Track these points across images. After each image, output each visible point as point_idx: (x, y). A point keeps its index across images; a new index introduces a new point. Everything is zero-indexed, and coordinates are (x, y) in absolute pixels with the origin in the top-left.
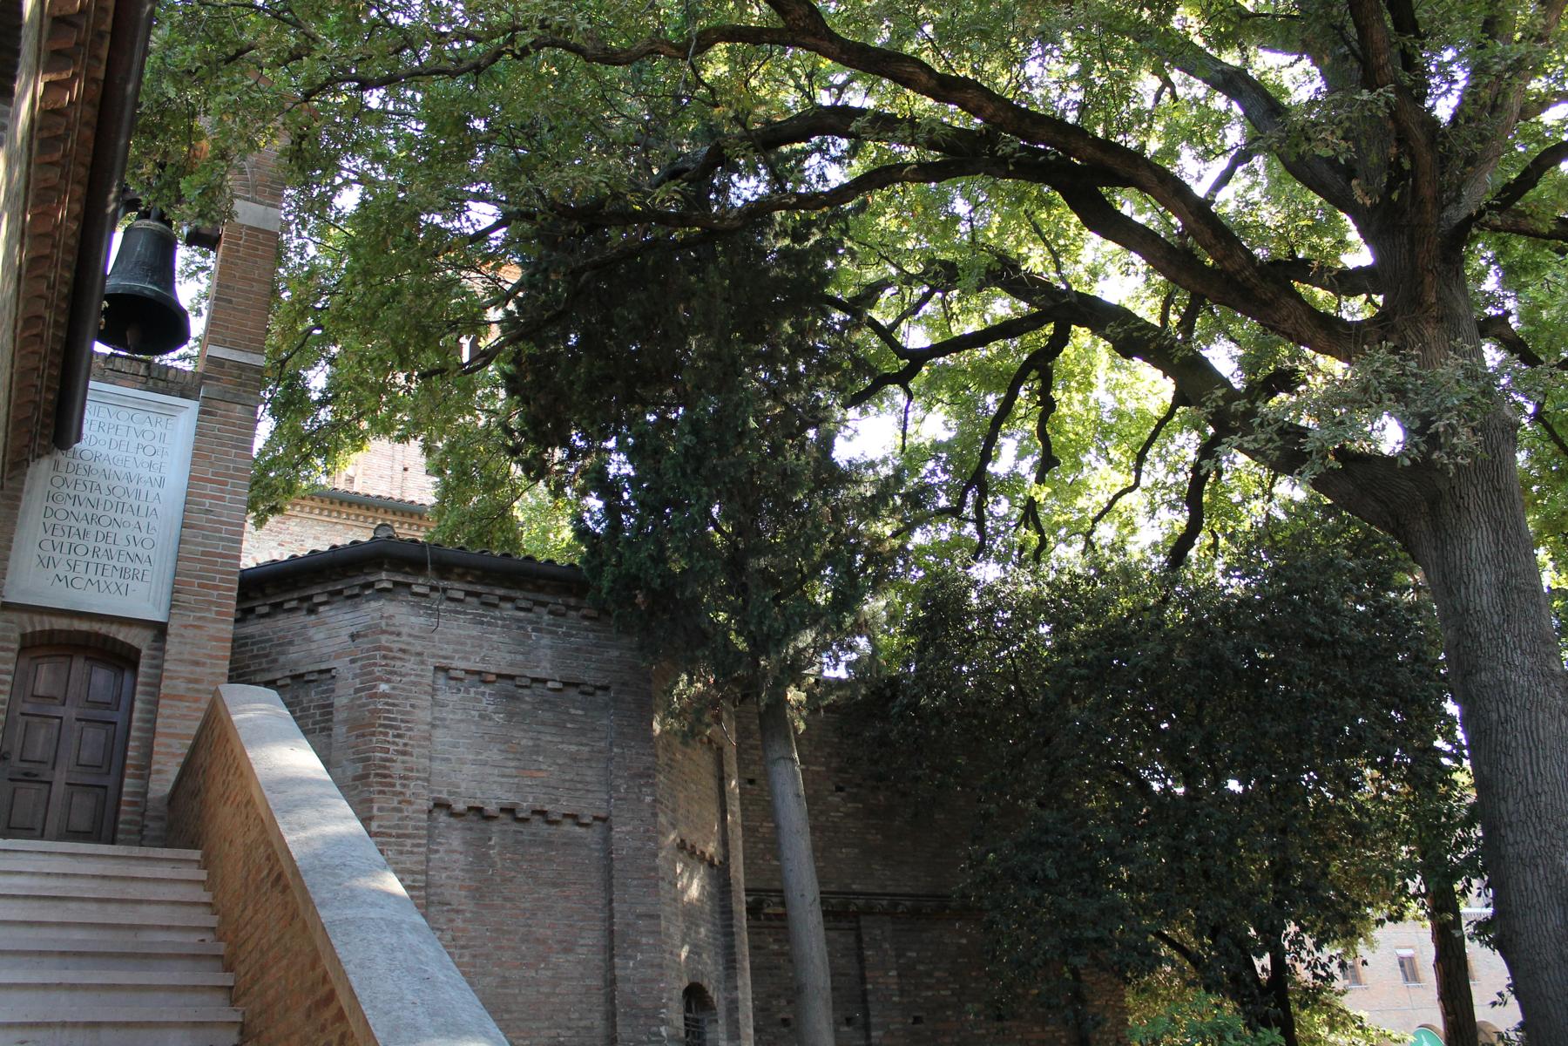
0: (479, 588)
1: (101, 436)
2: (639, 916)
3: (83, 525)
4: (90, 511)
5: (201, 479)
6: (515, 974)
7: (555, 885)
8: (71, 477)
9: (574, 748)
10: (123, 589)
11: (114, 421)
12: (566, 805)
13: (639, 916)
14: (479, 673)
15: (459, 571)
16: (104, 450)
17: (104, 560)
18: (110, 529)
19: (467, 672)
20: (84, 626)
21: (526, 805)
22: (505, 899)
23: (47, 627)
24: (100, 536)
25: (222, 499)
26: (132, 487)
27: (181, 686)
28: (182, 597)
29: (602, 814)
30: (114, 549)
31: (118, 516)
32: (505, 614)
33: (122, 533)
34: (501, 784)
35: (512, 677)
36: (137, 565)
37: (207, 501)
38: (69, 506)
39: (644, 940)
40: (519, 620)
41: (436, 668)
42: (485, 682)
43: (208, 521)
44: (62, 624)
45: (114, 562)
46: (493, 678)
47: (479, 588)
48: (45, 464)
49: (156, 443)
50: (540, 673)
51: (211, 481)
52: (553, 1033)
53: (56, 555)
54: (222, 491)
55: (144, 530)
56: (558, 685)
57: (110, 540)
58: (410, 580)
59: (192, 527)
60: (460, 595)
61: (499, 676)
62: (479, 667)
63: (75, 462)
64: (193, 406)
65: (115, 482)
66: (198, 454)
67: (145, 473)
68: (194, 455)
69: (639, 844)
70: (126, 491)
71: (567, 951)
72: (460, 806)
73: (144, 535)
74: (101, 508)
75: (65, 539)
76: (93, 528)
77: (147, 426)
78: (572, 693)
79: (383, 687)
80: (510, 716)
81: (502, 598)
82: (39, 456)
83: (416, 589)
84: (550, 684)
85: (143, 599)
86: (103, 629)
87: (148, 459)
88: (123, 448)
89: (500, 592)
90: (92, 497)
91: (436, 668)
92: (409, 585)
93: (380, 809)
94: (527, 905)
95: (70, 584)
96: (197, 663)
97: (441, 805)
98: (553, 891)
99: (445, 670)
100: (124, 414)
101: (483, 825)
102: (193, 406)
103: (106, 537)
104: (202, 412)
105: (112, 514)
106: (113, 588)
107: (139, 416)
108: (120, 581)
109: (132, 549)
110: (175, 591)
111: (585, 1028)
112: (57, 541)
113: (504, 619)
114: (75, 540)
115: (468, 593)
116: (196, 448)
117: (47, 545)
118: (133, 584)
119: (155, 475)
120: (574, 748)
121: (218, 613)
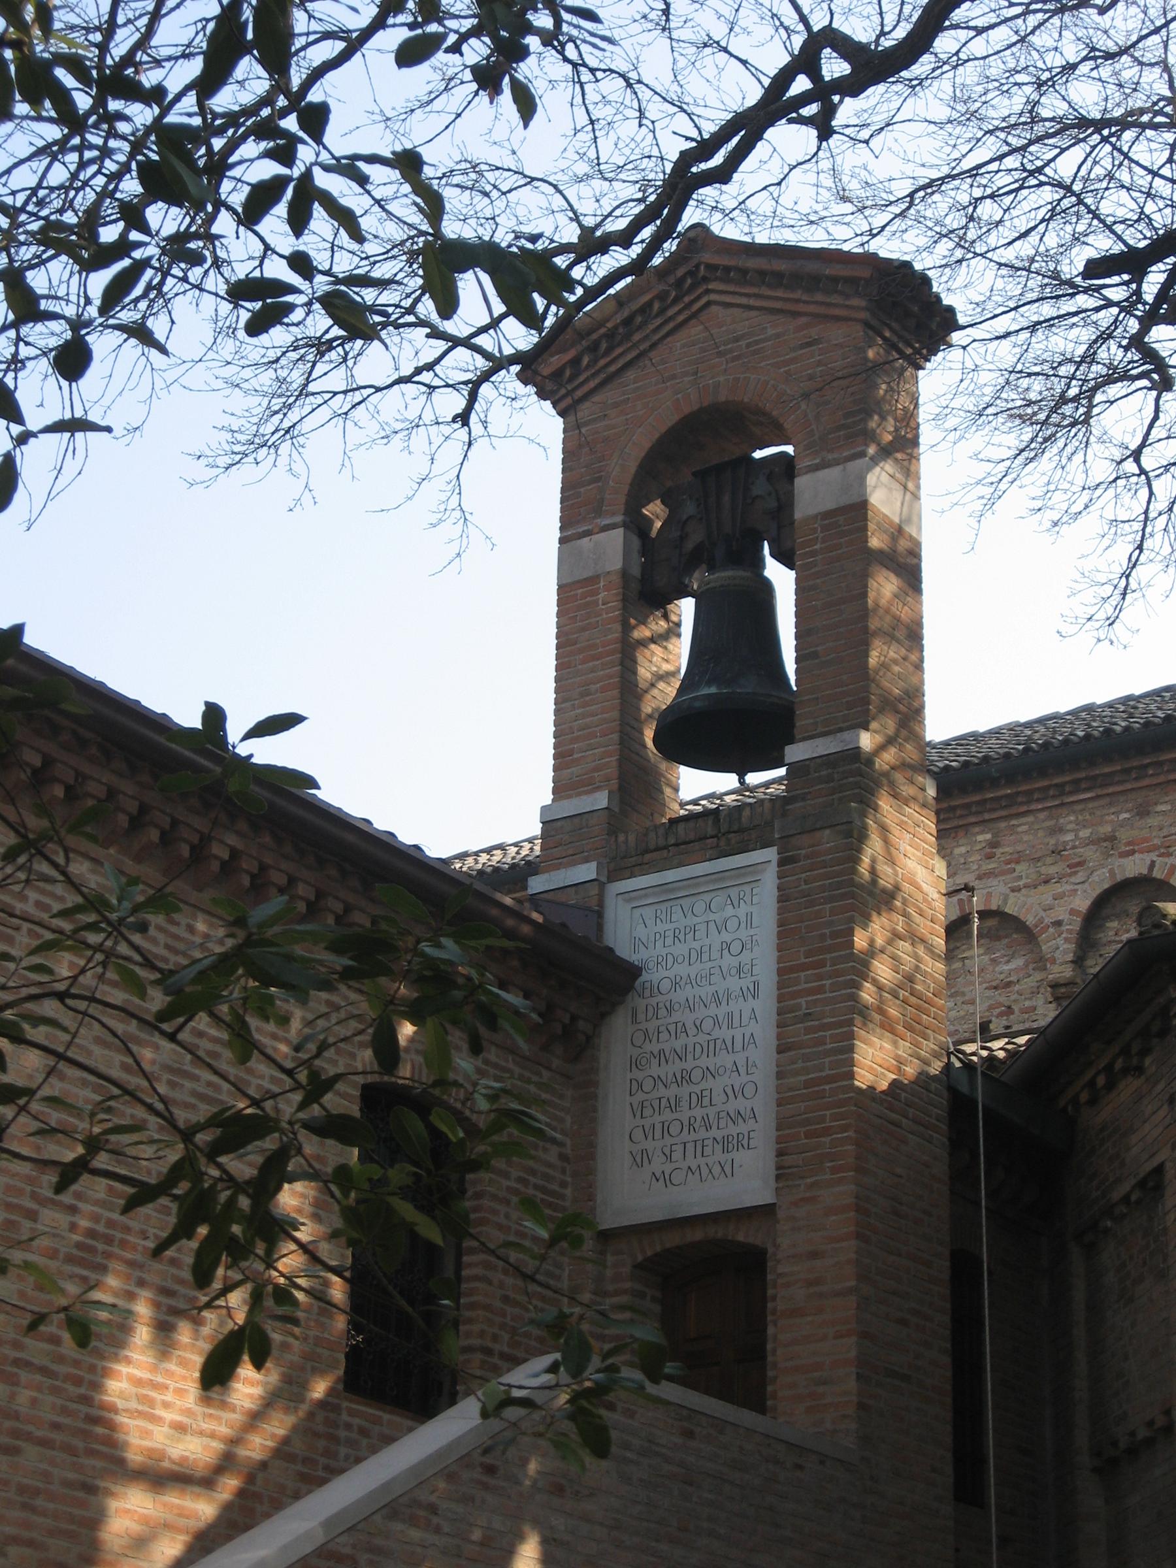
1: (680, 949)
3: (674, 1090)
4: (678, 1066)
5: (791, 969)
8: (651, 1026)
10: (728, 1169)
11: (691, 921)
16: (682, 970)
17: (702, 1134)
18: (703, 1085)
20: (697, 1235)
23: (658, 1249)
24: (694, 1097)
25: (820, 990)
26: (721, 1011)
28: (788, 1160)
30: (712, 1112)
31: (710, 1062)
33: (717, 1085)
36: (743, 1128)
37: (802, 1001)
38: (655, 1070)
43: (808, 1030)
44: (672, 1240)
45: (714, 1133)
49: (743, 934)
51: (803, 967)
53: (649, 1145)
54: (820, 977)
55: (742, 1070)
57: (706, 1101)
59: (789, 1049)
63: (653, 1001)
64: (770, 854)
65: (701, 1012)
66: (786, 932)
67: (734, 984)
68: (780, 936)
70: (716, 1021)
73: (744, 1078)
74: (690, 1057)
75: (657, 1119)
76: (686, 1089)
77: (729, 911)
82: (603, 1016)
85: (746, 1180)
87: (734, 962)
88: (705, 957)
90: (678, 1045)
95: (668, 1180)
96: (814, 1255)
100: (700, 907)
102: (770, 854)
103: (700, 1098)
104: (781, 863)
105: (704, 1062)
106: (717, 1170)
107: (719, 899)
108: (723, 1158)
109: (733, 1106)
110: (780, 1154)
112: (647, 1123)
114: (667, 1115)
116: (781, 924)
117: (638, 1135)
118: (741, 1156)
119: (747, 983)
121: (834, 1170)
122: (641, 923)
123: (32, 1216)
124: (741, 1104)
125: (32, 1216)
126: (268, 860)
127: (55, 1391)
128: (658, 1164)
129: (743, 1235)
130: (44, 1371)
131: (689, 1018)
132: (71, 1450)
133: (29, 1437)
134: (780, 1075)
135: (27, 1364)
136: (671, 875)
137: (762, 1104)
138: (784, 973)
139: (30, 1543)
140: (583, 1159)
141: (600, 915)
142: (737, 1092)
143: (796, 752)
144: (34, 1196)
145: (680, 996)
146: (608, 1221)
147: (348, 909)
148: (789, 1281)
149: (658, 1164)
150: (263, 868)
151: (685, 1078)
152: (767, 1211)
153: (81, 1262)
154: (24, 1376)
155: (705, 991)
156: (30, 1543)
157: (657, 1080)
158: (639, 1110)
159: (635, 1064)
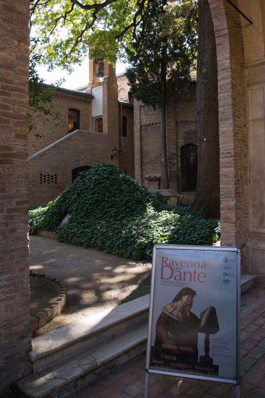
12: (156, 122)
20: (99, 117)
21: (152, 122)
44: (97, 118)
48: (93, 100)
64: (102, 86)
71: (158, 143)
86: (100, 117)
91: (140, 107)
96: (105, 119)
97: (142, 126)
98: (156, 135)
102: (102, 86)
120: (157, 112)
124: (100, 107)
128: (96, 112)
132: (44, 139)
137: (102, 107)
140: (89, 112)
141: (91, 92)
142: (100, 106)
146: (93, 117)
150: (56, 94)
151: (97, 105)
152: (102, 115)
157: (96, 105)
158: (94, 108)
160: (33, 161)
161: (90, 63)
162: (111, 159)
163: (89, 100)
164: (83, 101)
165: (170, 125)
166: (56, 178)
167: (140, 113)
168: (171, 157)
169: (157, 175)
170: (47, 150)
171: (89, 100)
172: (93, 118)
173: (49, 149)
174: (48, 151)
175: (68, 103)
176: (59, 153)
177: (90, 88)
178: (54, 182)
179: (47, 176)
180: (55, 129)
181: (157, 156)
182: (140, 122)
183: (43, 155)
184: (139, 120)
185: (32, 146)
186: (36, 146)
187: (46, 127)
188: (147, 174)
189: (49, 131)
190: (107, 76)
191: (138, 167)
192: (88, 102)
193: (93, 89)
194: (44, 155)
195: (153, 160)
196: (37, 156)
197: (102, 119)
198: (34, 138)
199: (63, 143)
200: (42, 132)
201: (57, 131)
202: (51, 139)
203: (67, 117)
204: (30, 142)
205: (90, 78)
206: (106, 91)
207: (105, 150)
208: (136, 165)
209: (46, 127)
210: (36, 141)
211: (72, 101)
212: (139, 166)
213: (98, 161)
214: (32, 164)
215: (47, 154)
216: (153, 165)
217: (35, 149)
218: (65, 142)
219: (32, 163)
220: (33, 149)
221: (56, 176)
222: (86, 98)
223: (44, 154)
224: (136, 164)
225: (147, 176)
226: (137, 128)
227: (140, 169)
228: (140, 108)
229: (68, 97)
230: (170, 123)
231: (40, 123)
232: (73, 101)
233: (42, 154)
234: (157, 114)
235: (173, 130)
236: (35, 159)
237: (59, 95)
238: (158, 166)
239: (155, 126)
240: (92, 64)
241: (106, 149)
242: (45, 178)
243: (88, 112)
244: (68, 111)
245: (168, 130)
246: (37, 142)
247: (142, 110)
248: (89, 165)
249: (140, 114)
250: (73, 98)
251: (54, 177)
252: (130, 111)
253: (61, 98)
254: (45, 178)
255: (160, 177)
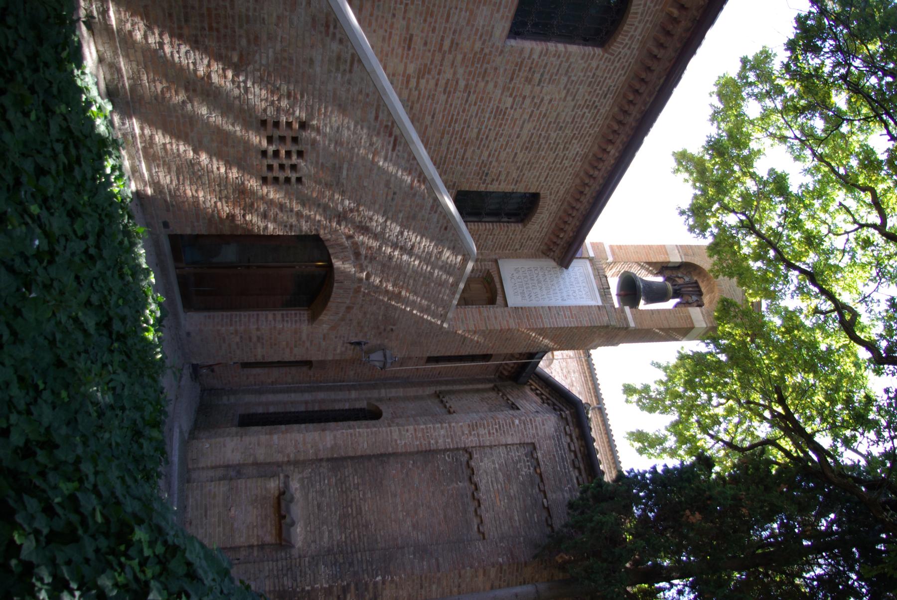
0: (579, 455)
2: (437, 560)
6: (398, 500)
7: (445, 517)
9: (516, 518)
12: (487, 516)
13: (437, 560)
14: (538, 464)
15: (583, 443)
16: (567, 280)
19: (537, 459)
20: (498, 286)
21: (482, 495)
22: (433, 493)
27: (485, 314)
29: (486, 536)
32: (572, 473)
34: (488, 482)
35: (542, 481)
36: (527, 297)
38: (541, 274)
39: (425, 563)
40: (572, 480)
41: (533, 444)
42: (535, 469)
44: (496, 279)
46: (538, 471)
47: (579, 455)
48: (554, 264)
50: (549, 495)
52: (372, 522)
56: (546, 504)
58: (571, 424)
60: (573, 448)
61: (541, 475)
62: (542, 463)
66: (581, 308)
67: (565, 294)
69: (475, 556)
72: (473, 464)
76: (536, 282)
78: (545, 514)
79: (517, 422)
80: (523, 483)
81: (579, 469)
83: (567, 428)
84: (545, 500)
85: (513, 300)
89: (582, 466)
91: (533, 444)
92: (568, 424)
93: (461, 426)
94: (432, 504)
96: (496, 318)
98: (442, 516)
99: (535, 448)
101: (466, 478)
102: (600, 303)
105: (544, 287)
109: (532, 294)
111: (376, 539)
113: (569, 472)
115: (575, 452)
119: (565, 298)
120: (516, 518)
122: (579, 269)
123: (511, 95)
124: (533, 297)
125: (511, 95)
126: (606, 163)
127: (461, 104)
128: (516, 275)
129: (499, 299)
130: (467, 101)
131: (555, 282)
133: (448, 97)
134: (542, 307)
135: (469, 95)
136: (592, 277)
138: (570, 308)
139: (419, 98)
140: (516, 255)
143: (627, 309)
144: (516, 96)
145: (560, 280)
146: (500, 262)
147: (590, 187)
148: (489, 311)
149: (516, 275)
150: (603, 161)
152: (506, 305)
153: (497, 111)
154: (466, 95)
155: (562, 287)
156: (419, 98)
158: (529, 269)
159: (542, 269)
160: (368, 95)
161: (663, 249)
162: (354, 340)
163: (557, 251)
164: (558, 236)
165: (477, 576)
166: (288, 180)
167: (513, 445)
168: (367, 589)
169: (298, 530)
170: (410, 153)
171: (557, 251)
172: (494, 264)
173: (414, 158)
174: (406, 155)
175: (561, 193)
176: (395, 193)
177: (592, 254)
178: (270, 175)
179: (294, 149)
180: (479, 148)
181: (367, 526)
182: (484, 447)
183: (390, 135)
184: (488, 443)
185: (426, 65)
186: (423, 82)
187: (489, 119)
188: (302, 480)
189: (476, 130)
190: (632, 324)
191: (329, 446)
192: (550, 250)
193: (588, 263)
194: (392, 139)
195: (351, 506)
196: (390, 114)
197: (492, 301)
198: (455, 73)
199: (432, 207)
200: (475, 104)
201: (469, 154)
202: (443, 134)
203: (512, 187)
204: (443, 59)
205: (620, 247)
206: (585, 323)
207: (391, 327)
208: (335, 437)
209: (489, 119)
210: (442, 82)
211: (566, 203)
212: (332, 448)
213: (349, 308)
214: (356, 90)
215: (393, 149)
216: (336, 509)
217: (409, 76)
218: (437, 215)
219: (361, 92)
220: (411, 68)
221: (293, 180)
222: (565, 246)
223: (395, 140)
224: (339, 434)
225: (295, 485)
226: (463, 434)
227: (322, 455)
228: (528, 444)
229: (581, 193)
230: (484, 575)
231: (510, 100)
232: (565, 205)
233: (396, 131)
234: (511, 519)
235: (459, 586)
236: (378, 106)
237: (595, 168)
238: (330, 532)
239: (471, 509)
240: (661, 258)
241: (392, 330)
242: (289, 140)
243: (517, 247)
244: (533, 190)
245: (460, 574)
246: (437, 85)
247: (523, 451)
248: (335, 285)
249: (506, 445)
250: (573, 208)
251: (293, 176)
252: (504, 369)
253: (582, 174)
254: (289, 140)
255: (293, 546)
